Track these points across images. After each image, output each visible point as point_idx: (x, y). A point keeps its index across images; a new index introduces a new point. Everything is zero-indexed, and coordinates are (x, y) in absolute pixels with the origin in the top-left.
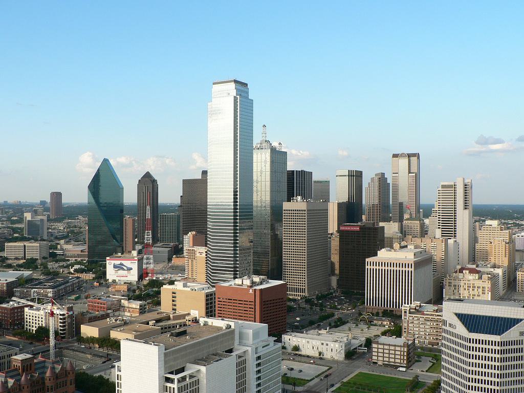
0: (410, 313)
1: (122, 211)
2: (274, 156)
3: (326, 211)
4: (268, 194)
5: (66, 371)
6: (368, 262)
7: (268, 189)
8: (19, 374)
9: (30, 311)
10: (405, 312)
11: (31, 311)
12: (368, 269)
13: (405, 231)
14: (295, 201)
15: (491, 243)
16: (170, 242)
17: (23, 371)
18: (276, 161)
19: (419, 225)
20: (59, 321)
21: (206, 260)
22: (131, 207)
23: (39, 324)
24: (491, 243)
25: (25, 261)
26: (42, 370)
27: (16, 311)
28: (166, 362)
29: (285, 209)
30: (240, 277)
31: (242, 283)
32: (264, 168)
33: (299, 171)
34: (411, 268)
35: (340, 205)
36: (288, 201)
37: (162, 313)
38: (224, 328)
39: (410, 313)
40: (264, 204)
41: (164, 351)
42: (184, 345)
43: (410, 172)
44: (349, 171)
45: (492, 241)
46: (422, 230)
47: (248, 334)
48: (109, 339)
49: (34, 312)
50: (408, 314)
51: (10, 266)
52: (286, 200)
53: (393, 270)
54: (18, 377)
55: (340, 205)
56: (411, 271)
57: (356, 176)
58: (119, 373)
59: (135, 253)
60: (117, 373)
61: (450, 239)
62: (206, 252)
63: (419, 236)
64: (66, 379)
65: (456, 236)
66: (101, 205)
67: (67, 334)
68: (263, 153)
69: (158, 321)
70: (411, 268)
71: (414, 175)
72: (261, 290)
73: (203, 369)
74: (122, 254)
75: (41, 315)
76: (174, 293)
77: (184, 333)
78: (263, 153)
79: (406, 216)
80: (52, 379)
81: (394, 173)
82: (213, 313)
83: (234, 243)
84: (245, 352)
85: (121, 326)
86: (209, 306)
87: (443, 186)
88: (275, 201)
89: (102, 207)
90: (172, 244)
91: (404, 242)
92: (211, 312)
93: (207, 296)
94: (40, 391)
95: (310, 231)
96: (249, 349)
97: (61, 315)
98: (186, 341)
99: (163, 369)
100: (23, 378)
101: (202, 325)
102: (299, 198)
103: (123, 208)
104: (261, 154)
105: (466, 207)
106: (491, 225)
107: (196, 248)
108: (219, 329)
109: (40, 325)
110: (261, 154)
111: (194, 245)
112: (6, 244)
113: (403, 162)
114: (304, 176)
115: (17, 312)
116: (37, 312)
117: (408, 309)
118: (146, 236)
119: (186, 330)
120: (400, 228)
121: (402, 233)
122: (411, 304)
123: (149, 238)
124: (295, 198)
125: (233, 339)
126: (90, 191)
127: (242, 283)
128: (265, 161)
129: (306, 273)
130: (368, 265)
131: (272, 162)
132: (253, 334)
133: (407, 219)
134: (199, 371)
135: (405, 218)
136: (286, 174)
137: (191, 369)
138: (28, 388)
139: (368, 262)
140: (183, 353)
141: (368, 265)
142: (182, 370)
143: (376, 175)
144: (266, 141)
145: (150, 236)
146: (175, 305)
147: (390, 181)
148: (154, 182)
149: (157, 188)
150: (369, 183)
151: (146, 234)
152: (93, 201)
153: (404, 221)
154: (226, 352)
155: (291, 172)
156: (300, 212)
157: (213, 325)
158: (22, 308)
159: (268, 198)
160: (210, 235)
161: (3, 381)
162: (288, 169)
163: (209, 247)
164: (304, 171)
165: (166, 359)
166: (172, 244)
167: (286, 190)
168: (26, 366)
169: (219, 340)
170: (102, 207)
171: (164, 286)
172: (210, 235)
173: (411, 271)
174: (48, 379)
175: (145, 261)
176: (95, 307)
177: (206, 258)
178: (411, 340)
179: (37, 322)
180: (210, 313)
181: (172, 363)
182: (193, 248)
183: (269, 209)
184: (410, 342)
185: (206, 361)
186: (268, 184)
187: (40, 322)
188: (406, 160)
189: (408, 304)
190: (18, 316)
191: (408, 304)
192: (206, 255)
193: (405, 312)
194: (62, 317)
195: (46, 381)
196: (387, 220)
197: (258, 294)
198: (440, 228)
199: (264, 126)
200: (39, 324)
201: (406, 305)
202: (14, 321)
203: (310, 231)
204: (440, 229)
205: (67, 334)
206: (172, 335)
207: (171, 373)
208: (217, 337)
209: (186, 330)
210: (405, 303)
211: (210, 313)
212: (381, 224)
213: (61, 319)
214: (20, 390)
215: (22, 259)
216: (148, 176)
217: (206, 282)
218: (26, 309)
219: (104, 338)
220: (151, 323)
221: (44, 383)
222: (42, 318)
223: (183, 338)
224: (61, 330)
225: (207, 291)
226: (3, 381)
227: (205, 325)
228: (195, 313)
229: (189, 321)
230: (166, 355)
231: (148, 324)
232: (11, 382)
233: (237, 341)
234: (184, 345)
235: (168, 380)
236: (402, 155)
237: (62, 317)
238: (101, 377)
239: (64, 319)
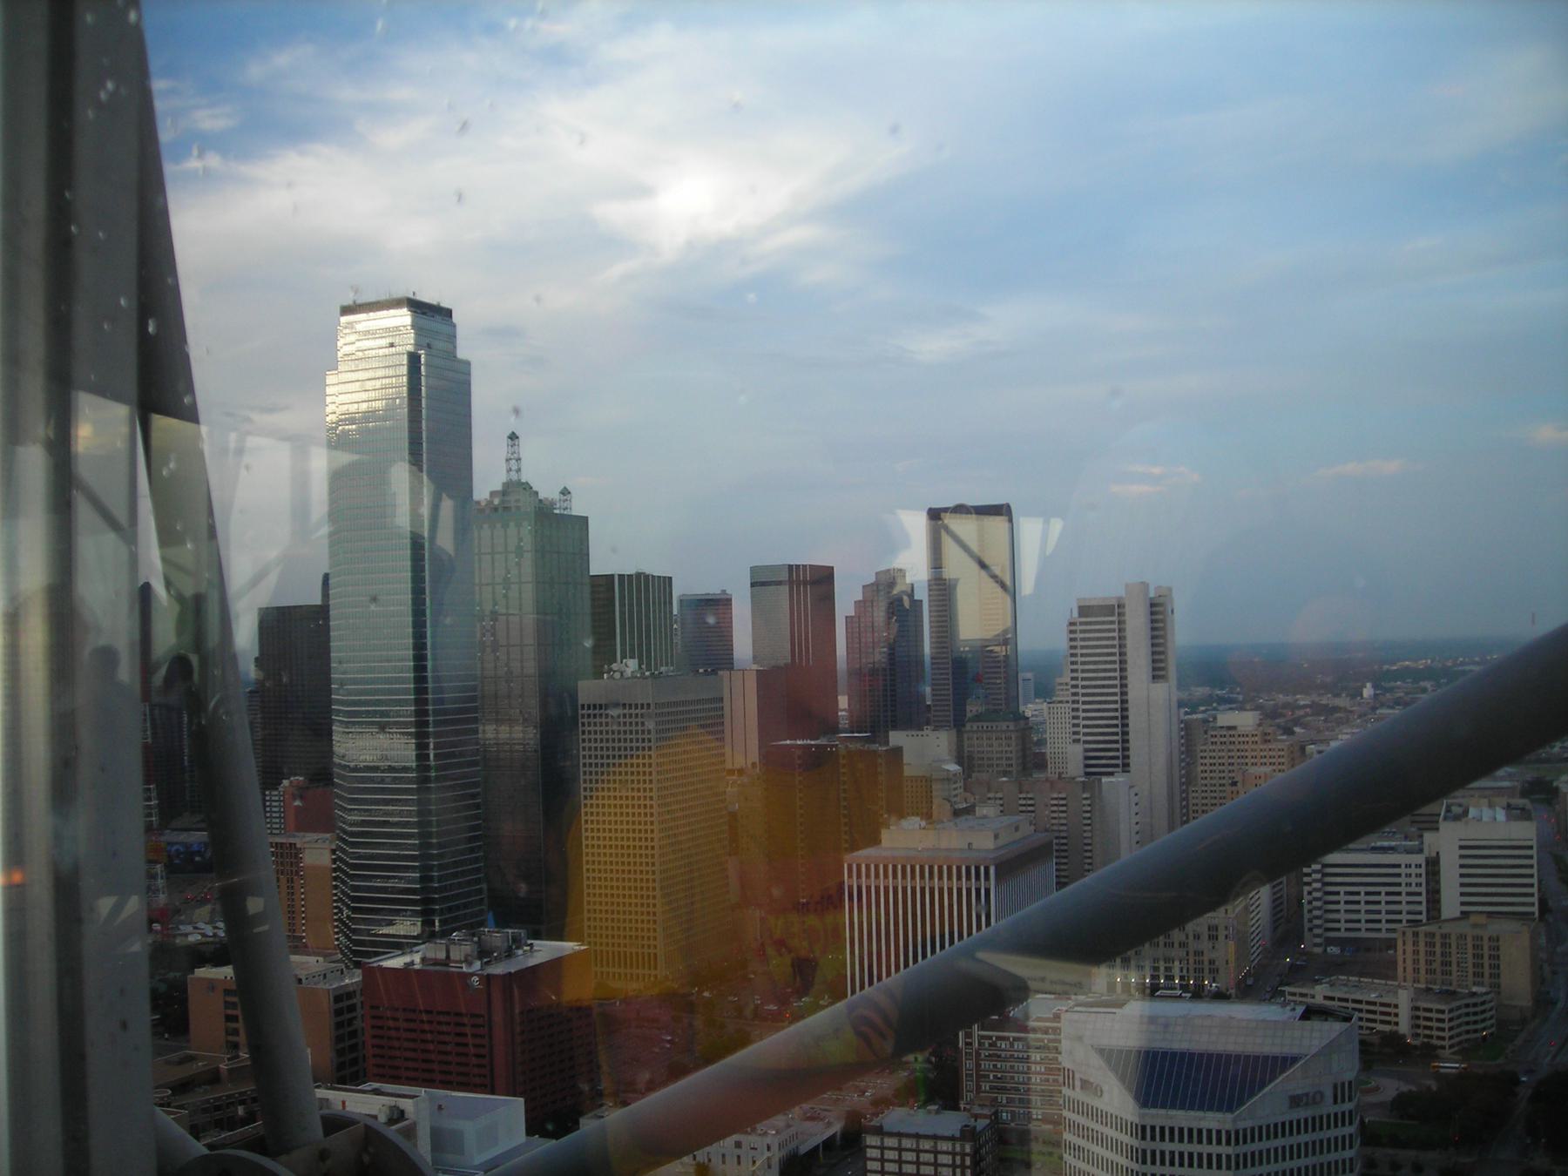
13: (971, 758)
14: (617, 675)
15: (1234, 784)
24: (1234, 784)
29: (586, 703)
33: (630, 576)
45: (1239, 778)
46: (1024, 756)
61: (1112, 774)
62: (333, 852)
65: (1128, 765)
68: (512, 524)
87: (1084, 610)
105: (1158, 674)
106: (1234, 728)
110: (505, 526)
121: (959, 761)
136: (587, 590)
162: (595, 569)
164: (647, 577)
182: (292, 840)
198: (1078, 741)
204: (1079, 748)
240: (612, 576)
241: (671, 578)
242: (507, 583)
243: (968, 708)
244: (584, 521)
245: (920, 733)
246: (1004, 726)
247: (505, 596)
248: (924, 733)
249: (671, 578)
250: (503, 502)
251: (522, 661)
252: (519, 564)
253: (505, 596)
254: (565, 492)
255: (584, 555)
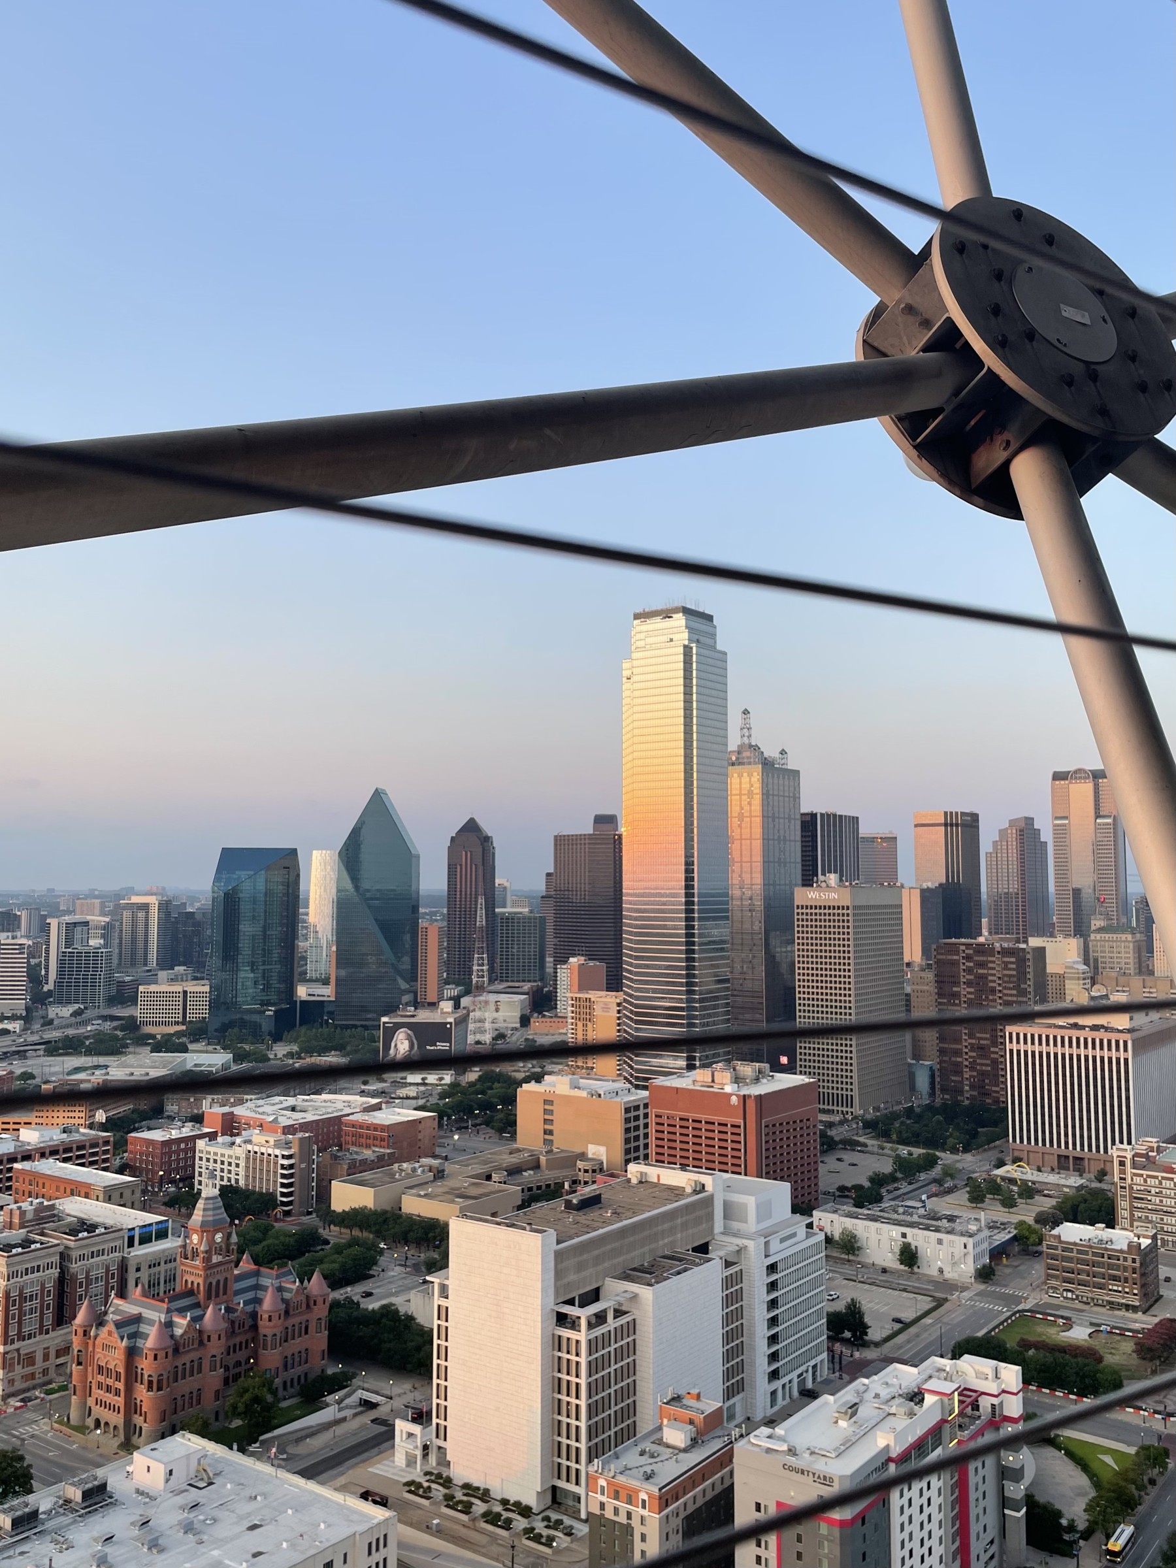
0: (1134, 1166)
1: (415, 909)
2: (770, 781)
3: (896, 910)
4: (758, 867)
5: (308, 1297)
6: (1011, 1034)
7: (758, 858)
8: (197, 1305)
9: (208, 1148)
10: (1122, 1164)
11: (212, 1149)
12: (1011, 1051)
13: (1096, 960)
16: (523, 981)
17: (209, 1298)
18: (776, 793)
19: (1131, 945)
20: (280, 1171)
21: (619, 1025)
22: (433, 900)
23: (229, 1180)
25: (184, 1028)
26: (250, 1295)
27: (183, 1146)
28: (559, 1274)
29: (800, 904)
30: (703, 1066)
31: (713, 1081)
32: (747, 808)
34: (1126, 1050)
35: (926, 895)
36: (804, 885)
37: (518, 1150)
38: (689, 1190)
39: (1134, 1166)
40: (748, 893)
41: (556, 1247)
42: (601, 1231)
43: (1098, 816)
44: (946, 813)
47: (745, 1205)
48: (400, 1216)
49: (220, 1151)
50: (1129, 1170)
51: (142, 1040)
52: (800, 882)
53: (1079, 1057)
54: (198, 1312)
55: (926, 895)
56: (1126, 1060)
57: (963, 825)
58: (443, 1302)
59: (447, 1006)
60: (437, 1301)
62: (619, 1005)
63: (1132, 972)
64: (304, 1318)
66: (368, 895)
67: (296, 1203)
68: (745, 775)
69: (514, 1171)
70: (1126, 1050)
71: (1109, 821)
72: (760, 1098)
73: (646, 1293)
74: (416, 1008)
75: (238, 1158)
76: (551, 1103)
77: (593, 1202)
78: (745, 775)
79: (1097, 923)
80: (275, 1316)
81: (1057, 818)
82: (642, 1152)
83: (688, 984)
84: (739, 1252)
85: (427, 1183)
86: (633, 1134)
88: (774, 885)
89: (372, 899)
90: (527, 986)
91: (1096, 987)
92: (637, 1149)
93: (627, 1110)
94: (234, 1351)
95: (861, 957)
96: (750, 1244)
97: (283, 1157)
98: (605, 1225)
99: (551, 1291)
100: (210, 1311)
101: (634, 1181)
102: (833, 878)
103: (418, 900)
104: (740, 776)
107: (593, 995)
108: (675, 1192)
109: (225, 1183)
110: (740, 776)
111: (582, 988)
112: (141, 988)
113: (1082, 791)
114: (841, 826)
115: (177, 1152)
116: (227, 1152)
117: (1129, 1155)
118: (475, 968)
119: (600, 1195)
120: (1082, 952)
121: (1086, 962)
122: (1129, 1143)
123: (482, 970)
124: (821, 878)
125: (710, 1217)
126: (342, 861)
127: (713, 1081)
128: (750, 794)
129: (855, 1064)
130: (1011, 1041)
131: (766, 795)
132: (758, 1206)
133: (1100, 930)
134: (635, 1297)
135: (1093, 928)
137: (616, 1290)
138: (219, 1339)
139: (1011, 1034)
140: (596, 1252)
141: (1011, 1041)
142: (594, 1296)
143: (1012, 823)
144: (750, 746)
145: (485, 968)
146: (550, 1133)
147: (1047, 836)
148: (486, 840)
149: (494, 854)
150: (995, 843)
151: (475, 962)
152: (349, 885)
153: (1092, 936)
154: (695, 1250)
155: (808, 818)
156: (831, 911)
157: (662, 1182)
158: (193, 1139)
159: (758, 879)
160: (631, 965)
161: (163, 1321)
162: (803, 810)
163: (626, 993)
165: (559, 1267)
166: (527, 986)
167: (799, 859)
168: (214, 1284)
169: (679, 1221)
170: (372, 899)
171: (524, 1085)
172: (631, 965)
173: (1126, 1060)
174: (266, 1316)
175: (471, 1026)
176: (361, 1136)
177: (619, 1018)
178: (1145, 1237)
179: (225, 1174)
180: (634, 1151)
181: (572, 1277)
182: (588, 996)
183: (759, 903)
184: (1145, 1242)
185: (650, 1273)
186: (758, 844)
187: (233, 1176)
188: (1088, 787)
189: (1129, 1143)
190: (178, 1160)
191: (1121, 1142)
192: (619, 1012)
193: (1122, 1164)
194: (286, 1162)
195: (260, 1323)
196: (1047, 930)
197: (751, 1106)
199: (746, 712)
200: (229, 1180)
201: (1125, 1146)
202: (168, 1172)
203: (861, 957)
205: (296, 1203)
206: (569, 1205)
207: (571, 1302)
208: (672, 1215)
209: (600, 1195)
210: (1121, 1142)
211: (634, 1151)
212: (1034, 942)
213: (283, 1167)
214: (201, 1343)
215: (177, 1023)
216: (471, 827)
217: (620, 1075)
218: (201, 1144)
219: (385, 1212)
220: (495, 1177)
221: (255, 1327)
222: (237, 1165)
223: (593, 1214)
224: (283, 1195)
225: (626, 1099)
226: (163, 1321)
227: (641, 1182)
228: (597, 1151)
229: (586, 1171)
230: (559, 1255)
231: (489, 1178)
232: (181, 1323)
233: (718, 1225)
234: (601, 1231)
235: (562, 1319)
236: (1078, 774)
237: (286, 1162)
238: (389, 1313)
239: (291, 1166)
240: (816, 814)
241: (857, 818)
242: (741, 817)
243: (1093, 922)
244: (796, 773)
245: (1054, 940)
246: (1123, 937)
247: (740, 826)
248: (1058, 939)
249: (857, 818)
250: (737, 759)
251: (751, 873)
252: (750, 804)
253: (740, 826)
254: (783, 752)
255: (796, 798)
